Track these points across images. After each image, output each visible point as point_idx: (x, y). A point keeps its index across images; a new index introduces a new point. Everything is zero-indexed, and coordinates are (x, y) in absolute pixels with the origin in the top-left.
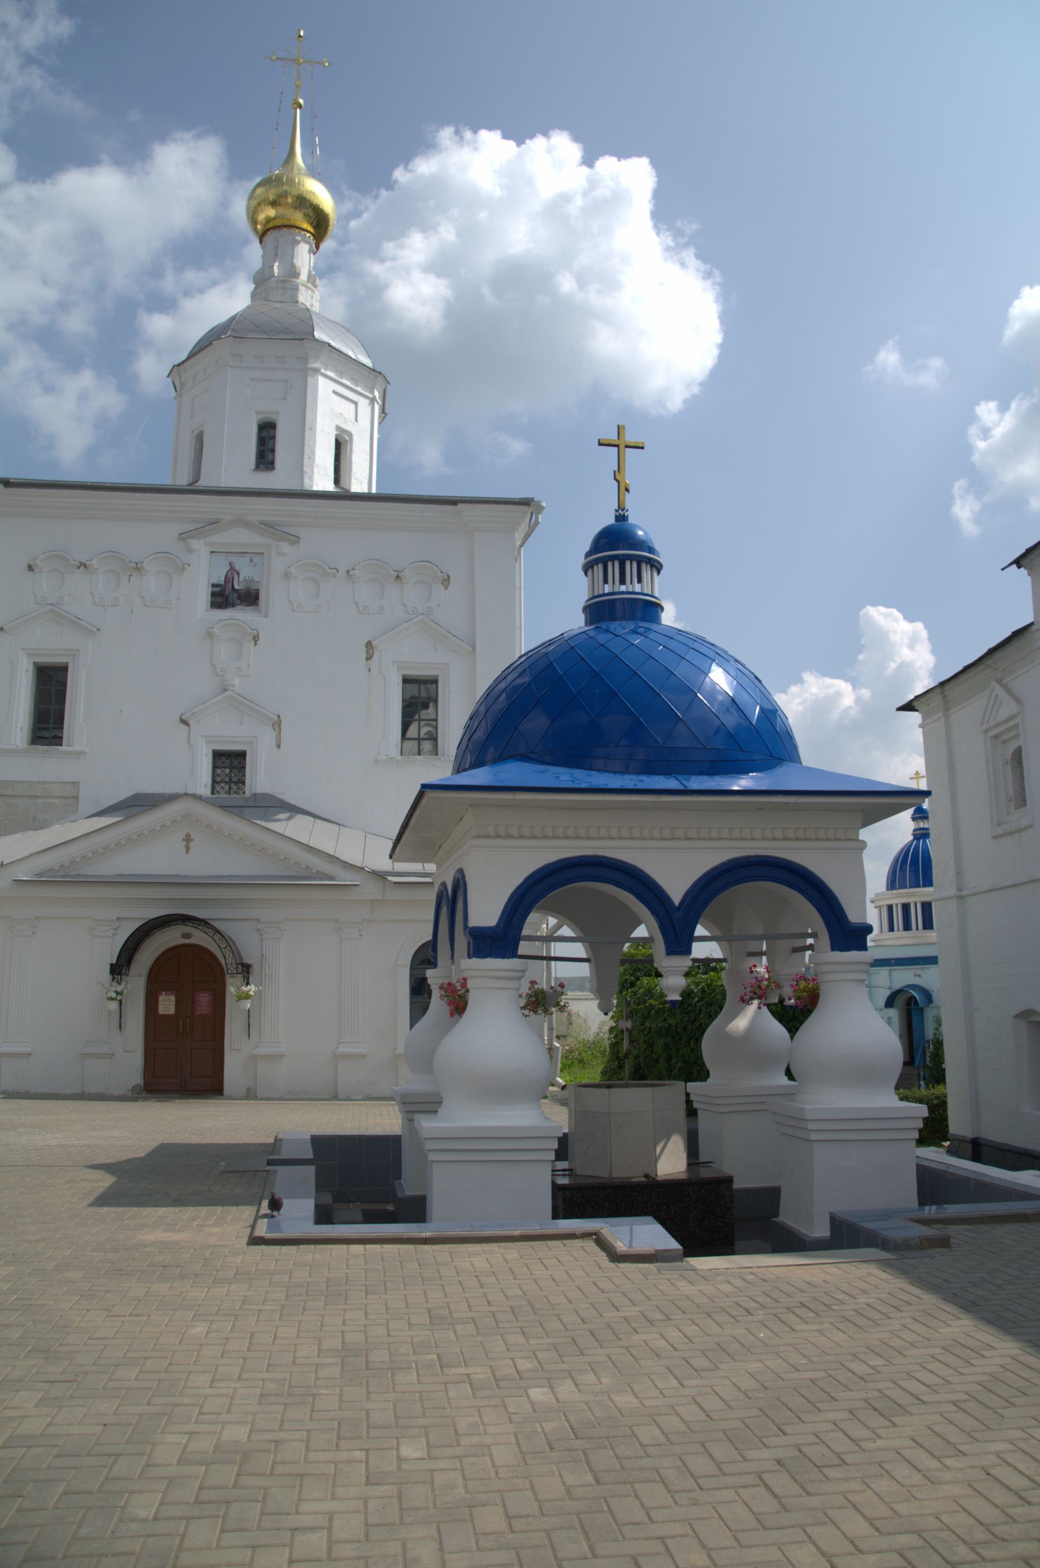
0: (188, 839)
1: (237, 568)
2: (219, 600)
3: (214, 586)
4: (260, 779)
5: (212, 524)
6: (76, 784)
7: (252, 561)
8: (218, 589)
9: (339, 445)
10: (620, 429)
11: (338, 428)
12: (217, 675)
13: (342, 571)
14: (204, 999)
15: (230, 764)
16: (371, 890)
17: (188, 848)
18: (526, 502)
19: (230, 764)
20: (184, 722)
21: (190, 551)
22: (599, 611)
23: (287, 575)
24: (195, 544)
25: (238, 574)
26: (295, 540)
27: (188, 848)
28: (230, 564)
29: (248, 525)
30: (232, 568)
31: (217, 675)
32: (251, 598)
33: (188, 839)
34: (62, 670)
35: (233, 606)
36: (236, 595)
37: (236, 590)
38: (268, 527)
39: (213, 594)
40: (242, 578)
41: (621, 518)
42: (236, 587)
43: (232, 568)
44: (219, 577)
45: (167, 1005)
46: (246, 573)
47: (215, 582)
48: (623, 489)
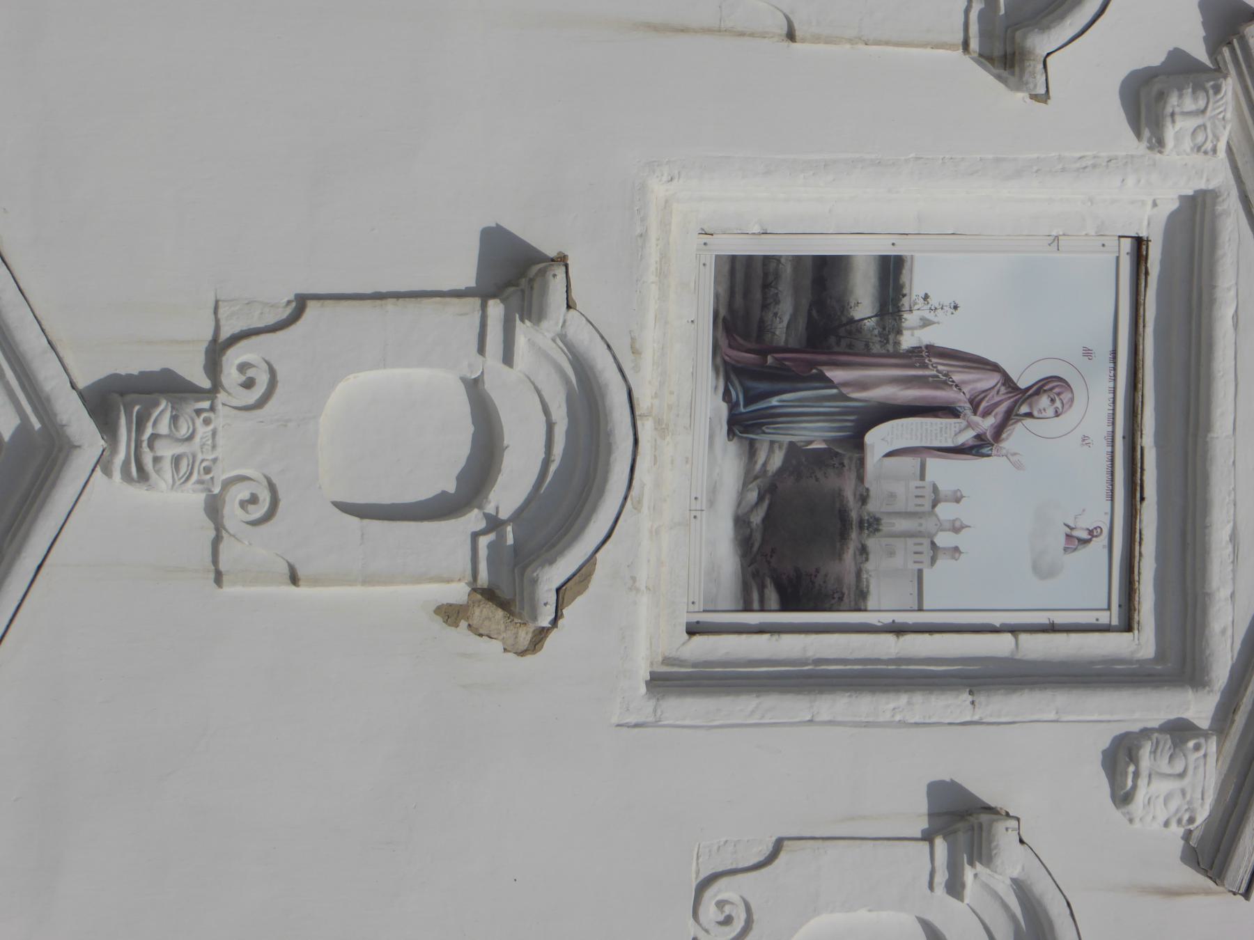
1: (1017, 437)
2: (784, 321)
3: (891, 270)
7: (1075, 542)
8: (863, 302)
12: (216, 351)
21: (1146, 99)
23: (962, 821)
25: (977, 448)
28: (1051, 386)
30: (1020, 399)
31: (216, 351)
35: (742, 425)
36: (815, 434)
37: (856, 442)
39: (825, 273)
40: (943, 472)
42: (880, 439)
43: (1020, 399)
44: (953, 309)
47: (919, 281)
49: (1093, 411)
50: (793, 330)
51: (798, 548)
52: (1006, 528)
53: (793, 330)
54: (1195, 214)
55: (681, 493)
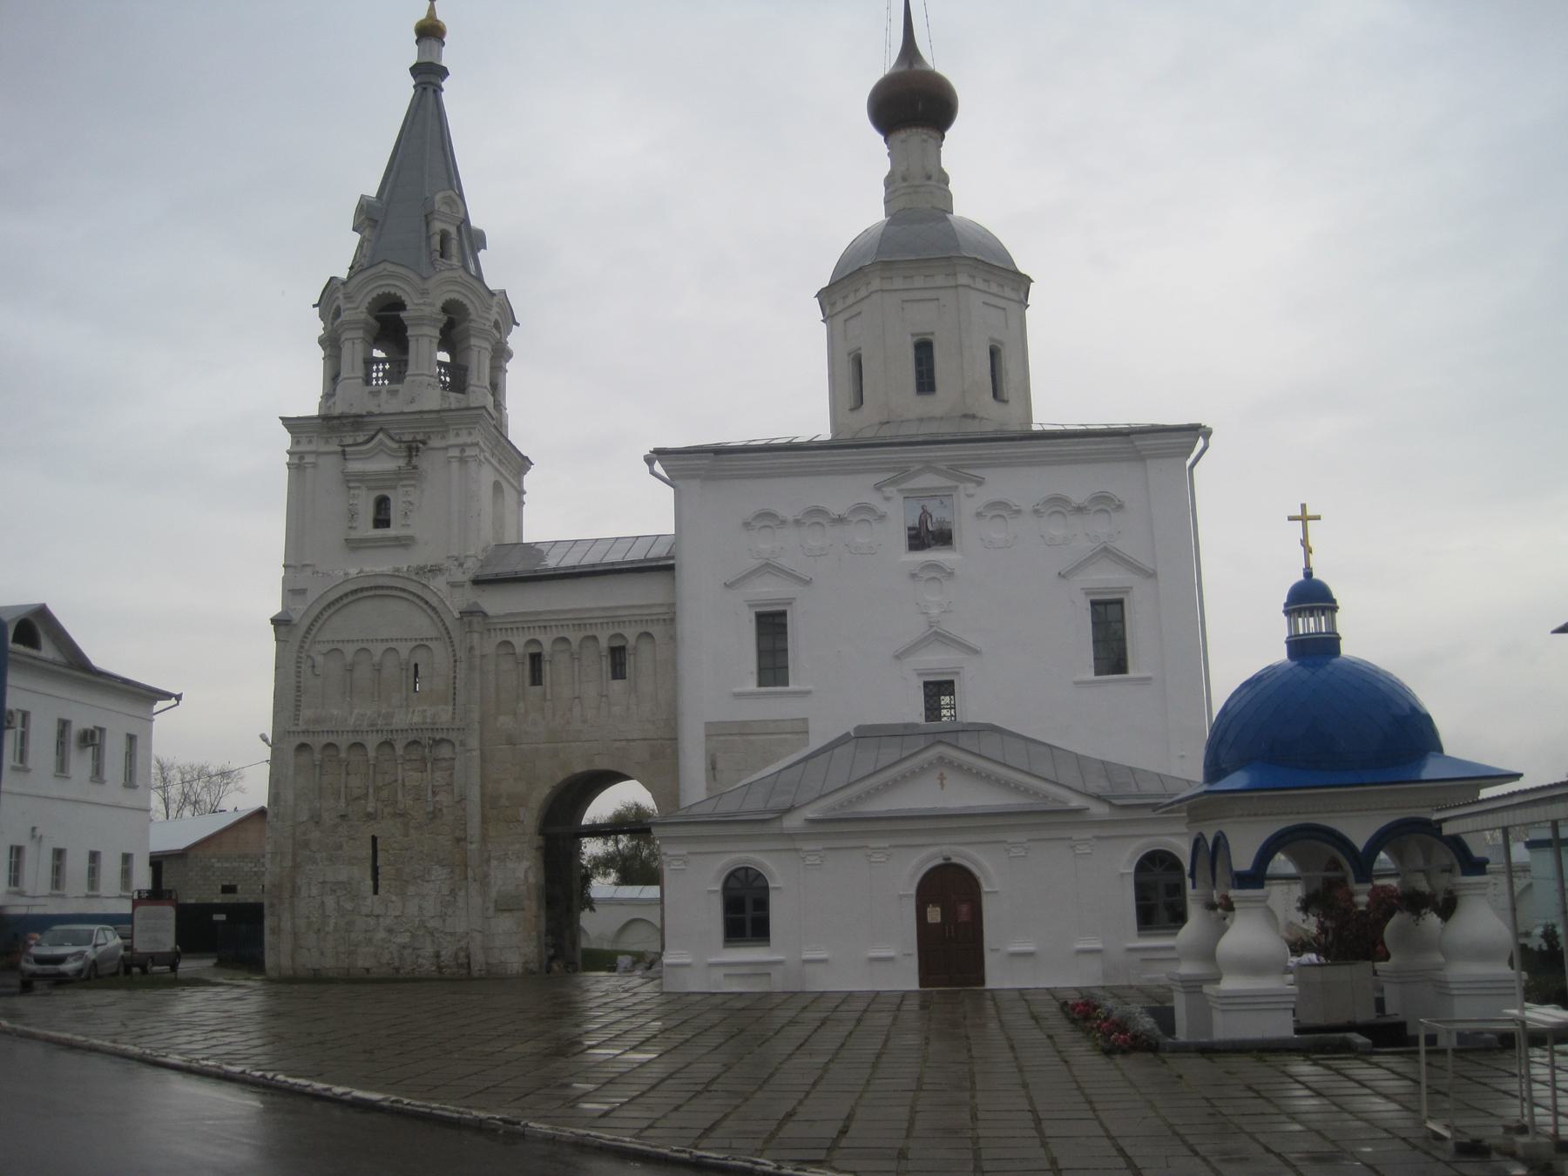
0: (942, 778)
4: (969, 706)
5: (904, 473)
6: (805, 720)
9: (994, 353)
10: (1303, 507)
11: (992, 339)
14: (964, 909)
16: (1099, 810)
17: (942, 785)
22: (1298, 646)
24: (890, 491)
26: (980, 482)
27: (942, 785)
29: (937, 472)
32: (944, 538)
33: (942, 778)
39: (910, 537)
41: (1308, 573)
45: (934, 915)
46: (938, 513)
48: (1308, 551)
49: (926, 502)
54: (900, 491)
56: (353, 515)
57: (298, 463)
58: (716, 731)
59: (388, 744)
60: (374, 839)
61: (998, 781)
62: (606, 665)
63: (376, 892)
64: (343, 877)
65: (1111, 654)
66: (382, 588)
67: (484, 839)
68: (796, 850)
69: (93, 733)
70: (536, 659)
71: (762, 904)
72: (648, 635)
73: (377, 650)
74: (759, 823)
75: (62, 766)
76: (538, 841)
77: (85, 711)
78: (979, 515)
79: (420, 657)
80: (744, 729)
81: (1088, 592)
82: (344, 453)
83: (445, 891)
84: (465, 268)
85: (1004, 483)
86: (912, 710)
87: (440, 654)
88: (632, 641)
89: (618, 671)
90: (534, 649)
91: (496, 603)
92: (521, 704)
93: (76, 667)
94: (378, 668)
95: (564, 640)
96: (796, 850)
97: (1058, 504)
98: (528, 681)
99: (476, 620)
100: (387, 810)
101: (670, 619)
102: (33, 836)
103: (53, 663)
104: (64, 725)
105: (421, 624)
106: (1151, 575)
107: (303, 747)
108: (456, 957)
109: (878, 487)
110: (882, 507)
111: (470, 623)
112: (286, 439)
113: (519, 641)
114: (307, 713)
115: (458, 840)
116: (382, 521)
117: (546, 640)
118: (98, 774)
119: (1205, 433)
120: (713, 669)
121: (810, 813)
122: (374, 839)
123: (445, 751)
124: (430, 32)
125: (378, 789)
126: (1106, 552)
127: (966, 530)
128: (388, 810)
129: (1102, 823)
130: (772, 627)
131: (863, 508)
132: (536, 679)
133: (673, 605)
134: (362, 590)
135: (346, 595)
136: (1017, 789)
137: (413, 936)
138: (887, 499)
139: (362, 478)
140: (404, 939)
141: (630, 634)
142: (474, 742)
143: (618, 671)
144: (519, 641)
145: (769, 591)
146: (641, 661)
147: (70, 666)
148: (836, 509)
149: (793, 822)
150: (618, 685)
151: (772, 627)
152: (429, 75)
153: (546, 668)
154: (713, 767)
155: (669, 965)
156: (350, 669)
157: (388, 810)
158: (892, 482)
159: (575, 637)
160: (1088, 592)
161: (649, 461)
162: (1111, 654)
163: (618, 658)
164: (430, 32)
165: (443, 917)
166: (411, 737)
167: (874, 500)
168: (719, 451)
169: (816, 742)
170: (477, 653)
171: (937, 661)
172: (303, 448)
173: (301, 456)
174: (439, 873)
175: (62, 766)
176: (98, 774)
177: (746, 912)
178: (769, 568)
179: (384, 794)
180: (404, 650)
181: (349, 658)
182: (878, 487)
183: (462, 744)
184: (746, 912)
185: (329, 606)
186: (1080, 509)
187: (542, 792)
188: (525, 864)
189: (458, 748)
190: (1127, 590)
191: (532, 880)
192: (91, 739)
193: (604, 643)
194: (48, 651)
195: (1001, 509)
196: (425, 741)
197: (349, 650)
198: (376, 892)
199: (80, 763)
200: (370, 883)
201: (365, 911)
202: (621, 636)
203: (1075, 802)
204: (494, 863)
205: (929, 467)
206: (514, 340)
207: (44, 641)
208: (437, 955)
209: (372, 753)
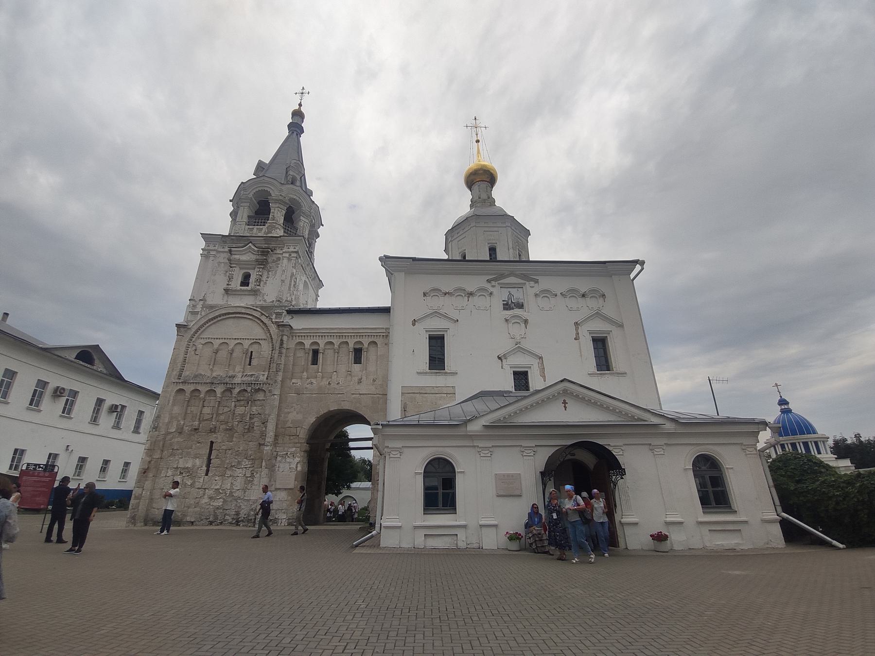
0: (565, 403)
4: (535, 382)
5: (502, 276)
13: (559, 294)
15: (521, 378)
17: (565, 407)
18: (636, 262)
19: (521, 378)
20: (499, 358)
24: (493, 283)
26: (537, 282)
27: (565, 407)
29: (516, 276)
33: (565, 403)
34: (441, 338)
38: (526, 277)
50: (507, 306)
51: (521, 306)
52: (517, 295)
53: (507, 306)
55: (517, 311)
56: (230, 279)
57: (206, 254)
58: (408, 393)
59: (229, 390)
60: (212, 443)
61: (601, 406)
62: (352, 356)
63: (207, 474)
64: (189, 465)
65: (604, 363)
66: (240, 313)
67: (275, 443)
68: (474, 446)
69: (117, 406)
70: (316, 353)
71: (449, 483)
72: (375, 343)
73: (232, 344)
74: (454, 428)
75: (94, 420)
76: (306, 447)
77: (113, 397)
78: (536, 295)
79: (255, 348)
80: (422, 391)
81: (590, 332)
82: (230, 251)
83: (248, 475)
84: (301, 187)
85: (545, 283)
86: (508, 384)
87: (266, 347)
88: (366, 345)
89: (358, 360)
90: (315, 347)
91: (298, 323)
92: (305, 374)
93: (114, 376)
94: (231, 352)
95: (331, 343)
96: (474, 446)
97: (572, 293)
98: (310, 363)
99: (287, 329)
100: (222, 427)
101: (387, 336)
102: (67, 449)
103: (101, 372)
104: (100, 402)
105: (258, 332)
106: (621, 326)
107: (181, 391)
108: (249, 515)
109: (489, 281)
110: (491, 289)
111: (283, 331)
112: (202, 244)
113: (307, 343)
114: (186, 373)
115: (260, 445)
116: (245, 282)
117: (322, 343)
118: (117, 426)
119: (642, 263)
120: (405, 363)
121: (484, 421)
122: (212, 443)
123: (260, 396)
124: (298, 115)
125: (218, 415)
126: (598, 315)
127: (531, 303)
128: (224, 427)
129: (670, 435)
130: (437, 343)
131: (482, 289)
132: (315, 361)
133: (388, 329)
134: (229, 313)
135: (220, 316)
136: (613, 411)
137: (225, 501)
138: (493, 286)
139: (239, 263)
140: (219, 503)
141: (366, 342)
142: (277, 392)
143: (358, 360)
144: (307, 343)
145: (436, 325)
146: (370, 356)
147: (111, 375)
148: (470, 289)
149: (475, 427)
150: (357, 367)
151: (437, 343)
152: (296, 127)
153: (320, 356)
154: (404, 410)
155: (387, 527)
156: (216, 352)
157: (224, 427)
158: (495, 279)
159: (336, 342)
160: (590, 332)
161: (380, 259)
162: (604, 363)
163: (358, 355)
164: (298, 115)
165: (244, 490)
166: (244, 387)
167: (488, 286)
168: (414, 259)
169: (460, 398)
170: (285, 346)
171: (520, 361)
172: (211, 247)
173: (209, 251)
174: (246, 463)
175: (94, 420)
176: (117, 426)
177: (440, 491)
178: (436, 314)
179: (222, 417)
180: (246, 344)
181: (216, 346)
182: (489, 281)
183: (270, 391)
184: (440, 491)
185: (210, 320)
186: (583, 296)
187: (312, 419)
188: (297, 459)
189: (268, 394)
190: (609, 332)
191: (299, 468)
192: (117, 410)
193: (351, 345)
194: (99, 366)
195: (546, 293)
196: (249, 389)
197: (216, 343)
198: (207, 474)
199: (106, 421)
200: (205, 468)
201: (198, 485)
202: (360, 343)
203: (655, 420)
204: (279, 459)
205: (512, 274)
206: (320, 230)
207: (97, 362)
208: (238, 514)
209: (219, 395)
